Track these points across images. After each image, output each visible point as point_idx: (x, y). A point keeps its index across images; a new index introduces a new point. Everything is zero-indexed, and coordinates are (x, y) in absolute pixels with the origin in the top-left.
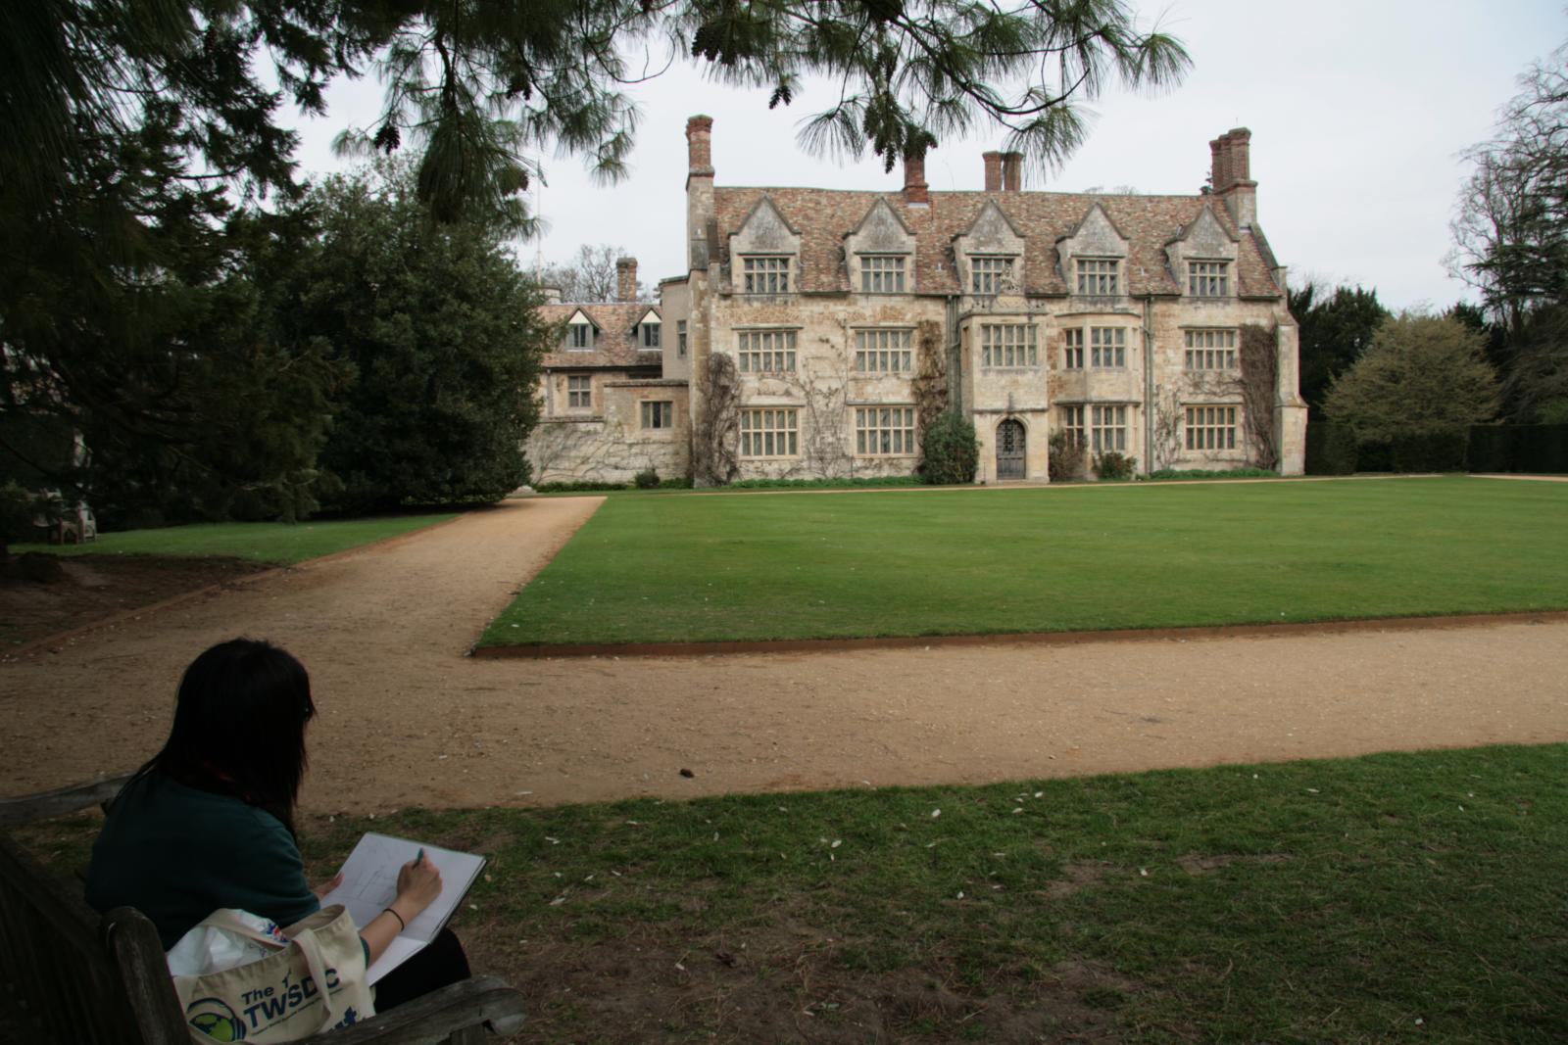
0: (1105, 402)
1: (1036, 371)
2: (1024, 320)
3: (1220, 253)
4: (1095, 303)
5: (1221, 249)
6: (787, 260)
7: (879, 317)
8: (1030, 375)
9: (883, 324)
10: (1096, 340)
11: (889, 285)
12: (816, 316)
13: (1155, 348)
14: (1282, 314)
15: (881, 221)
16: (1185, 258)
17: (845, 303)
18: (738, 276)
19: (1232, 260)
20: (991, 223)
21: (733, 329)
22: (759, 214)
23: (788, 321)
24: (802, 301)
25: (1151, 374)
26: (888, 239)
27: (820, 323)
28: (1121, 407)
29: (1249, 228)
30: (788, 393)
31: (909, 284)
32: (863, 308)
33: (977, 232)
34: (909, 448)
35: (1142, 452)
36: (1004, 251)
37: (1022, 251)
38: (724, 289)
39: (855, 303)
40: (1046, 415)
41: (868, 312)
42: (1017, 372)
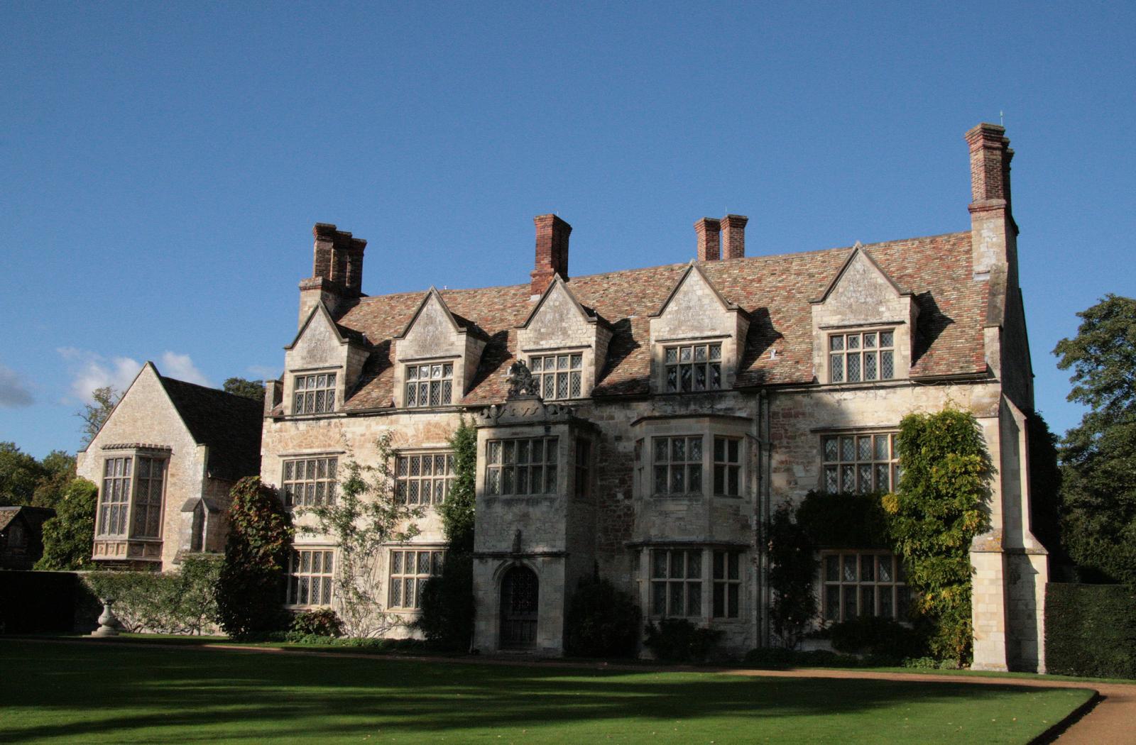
0: (665, 544)
1: (552, 501)
2: (539, 431)
3: (879, 314)
4: (687, 405)
5: (882, 309)
6: (334, 374)
7: (421, 436)
8: (544, 506)
9: (425, 445)
10: (659, 456)
11: (434, 399)
12: (358, 438)
13: (774, 463)
14: (986, 400)
15: (431, 321)
16: (820, 328)
17: (387, 421)
18: (288, 396)
19: (903, 322)
20: (556, 309)
21: (280, 456)
22: (312, 324)
23: (330, 445)
24: (344, 420)
25: (768, 500)
26: (436, 341)
27: (361, 446)
28: (694, 550)
29: (989, 272)
30: (325, 530)
31: (457, 392)
32: (405, 426)
33: (537, 321)
34: (407, 604)
35: (754, 621)
36: (568, 345)
37: (592, 340)
38: (273, 411)
39: (397, 422)
40: (563, 561)
41: (410, 432)
42: (529, 502)
